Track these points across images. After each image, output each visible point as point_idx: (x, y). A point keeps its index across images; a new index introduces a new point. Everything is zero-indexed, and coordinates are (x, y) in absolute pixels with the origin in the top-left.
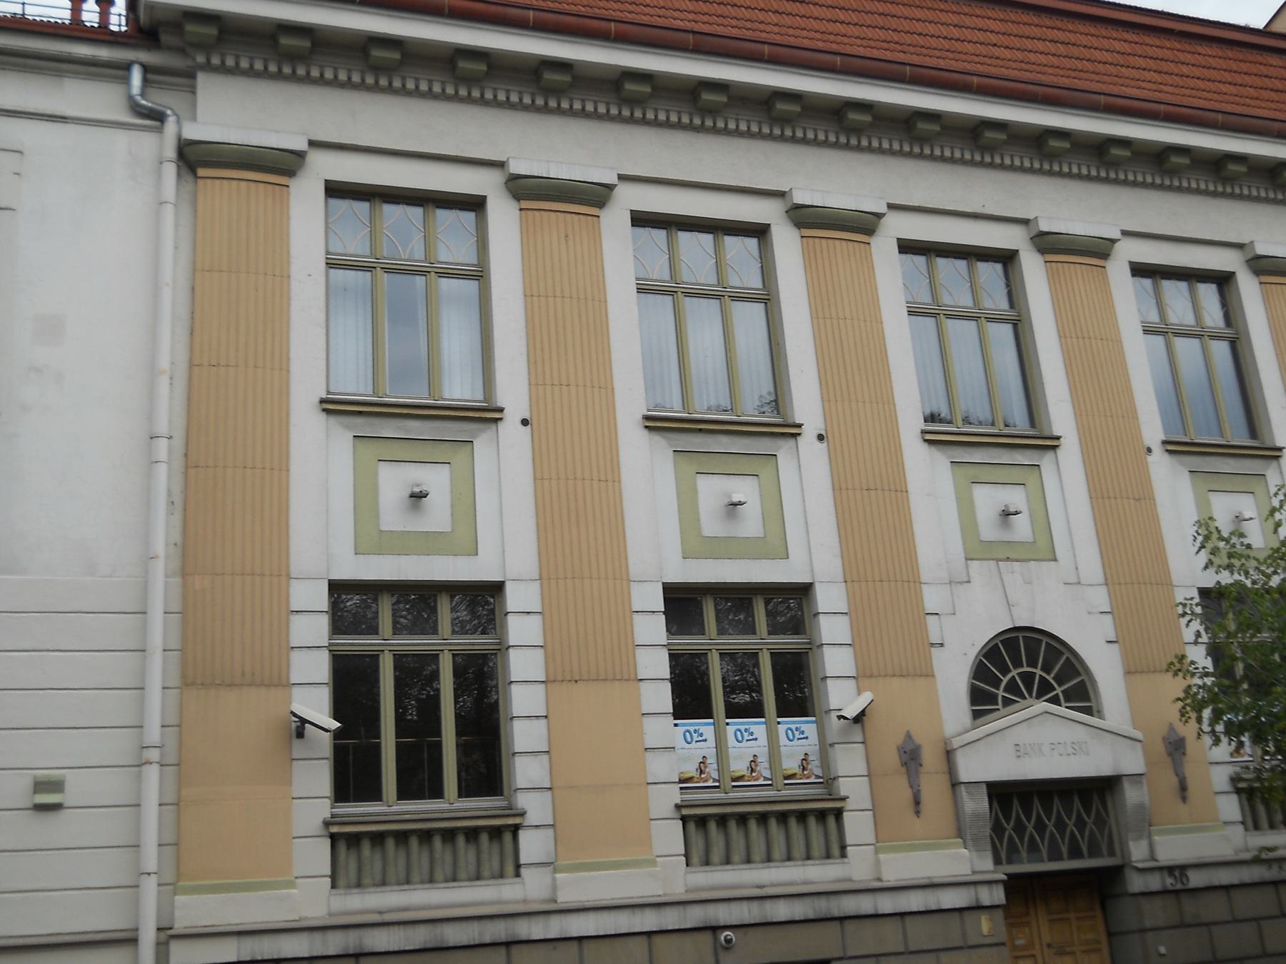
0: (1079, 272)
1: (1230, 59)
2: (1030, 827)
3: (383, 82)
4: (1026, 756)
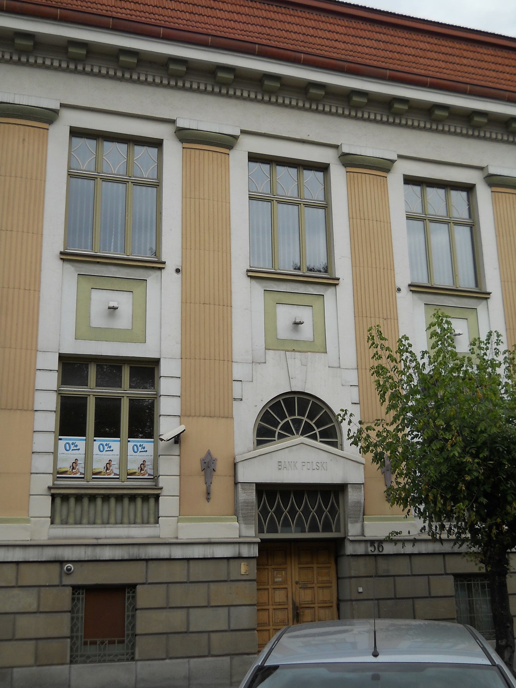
0: (372, 180)
1: (499, 57)
2: (313, 512)
3: (24, 59)
4: (285, 469)
